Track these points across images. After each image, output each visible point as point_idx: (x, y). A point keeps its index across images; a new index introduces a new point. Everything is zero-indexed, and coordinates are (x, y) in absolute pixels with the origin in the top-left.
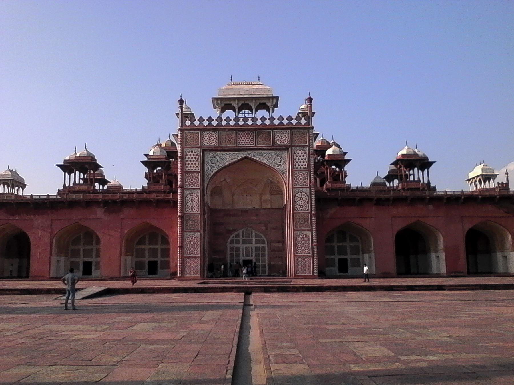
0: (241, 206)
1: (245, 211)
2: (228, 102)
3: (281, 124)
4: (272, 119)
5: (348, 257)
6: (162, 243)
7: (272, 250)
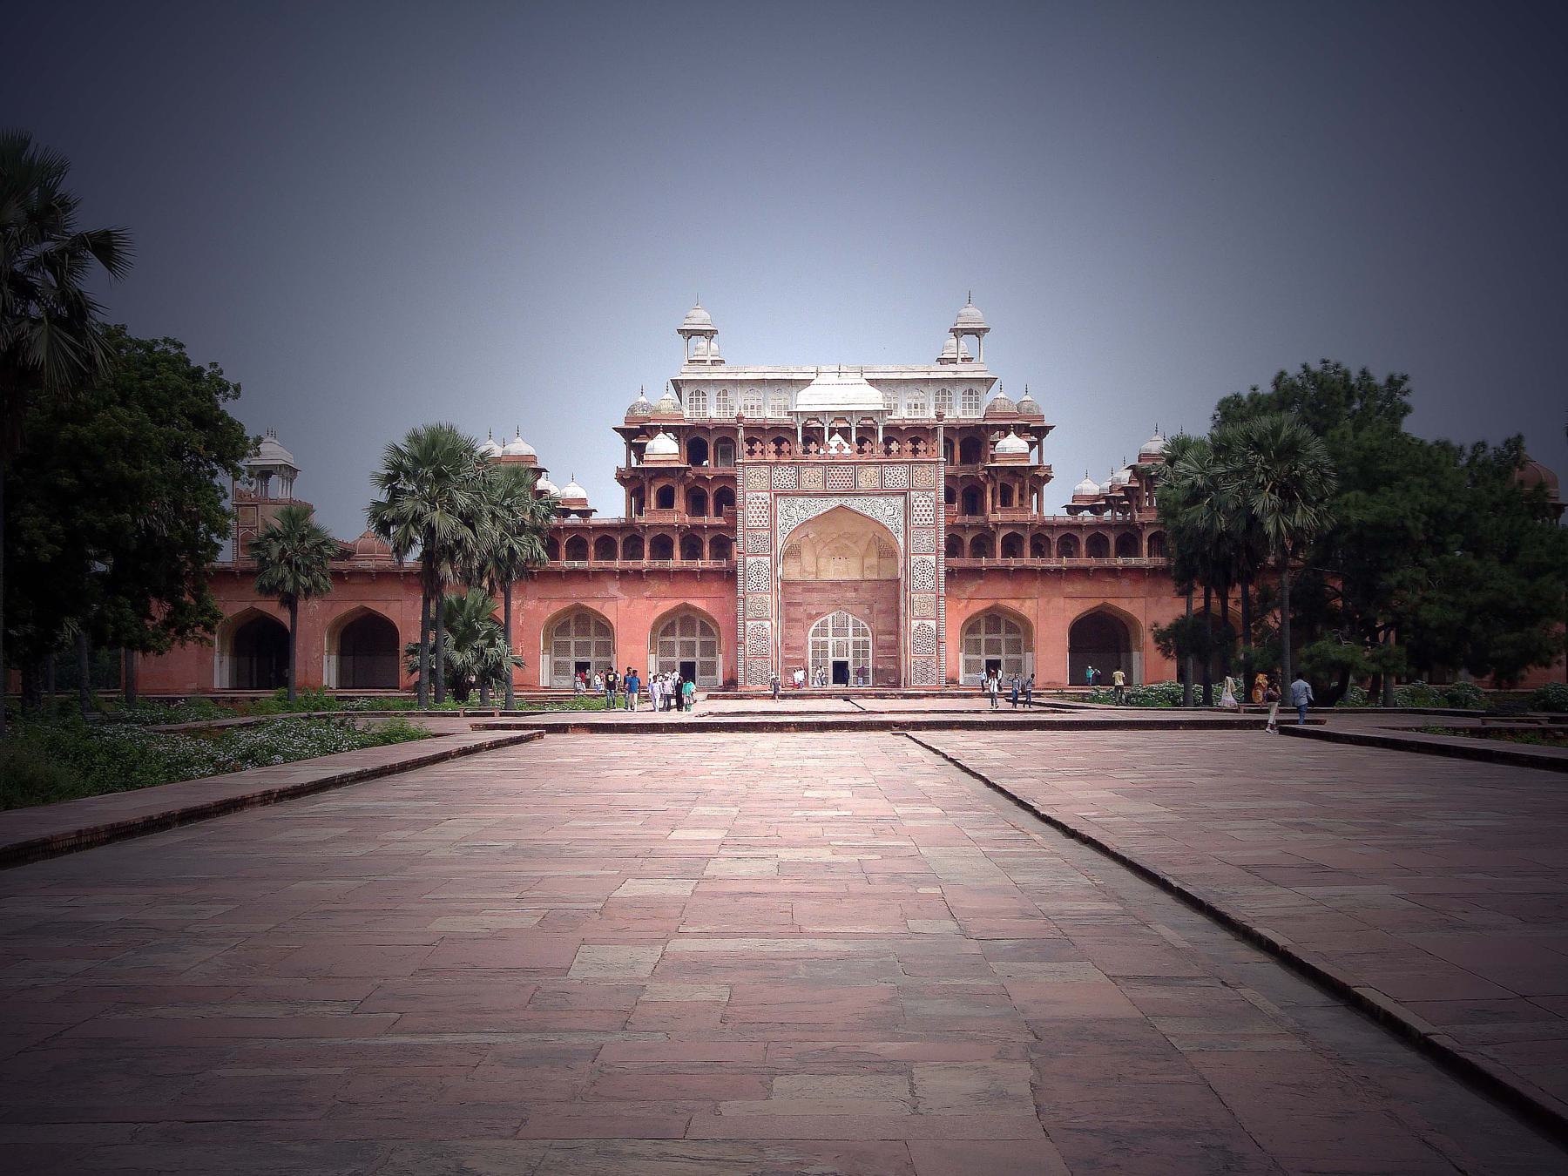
1: (837, 584)
5: (1002, 657)
7: (879, 646)
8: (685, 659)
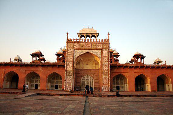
0: (86, 68)
1: (87, 70)
2: (83, 34)
3: (99, 42)
4: (96, 40)
5: (120, 85)
6: (60, 79)
7: (95, 83)
8: (56, 84)
